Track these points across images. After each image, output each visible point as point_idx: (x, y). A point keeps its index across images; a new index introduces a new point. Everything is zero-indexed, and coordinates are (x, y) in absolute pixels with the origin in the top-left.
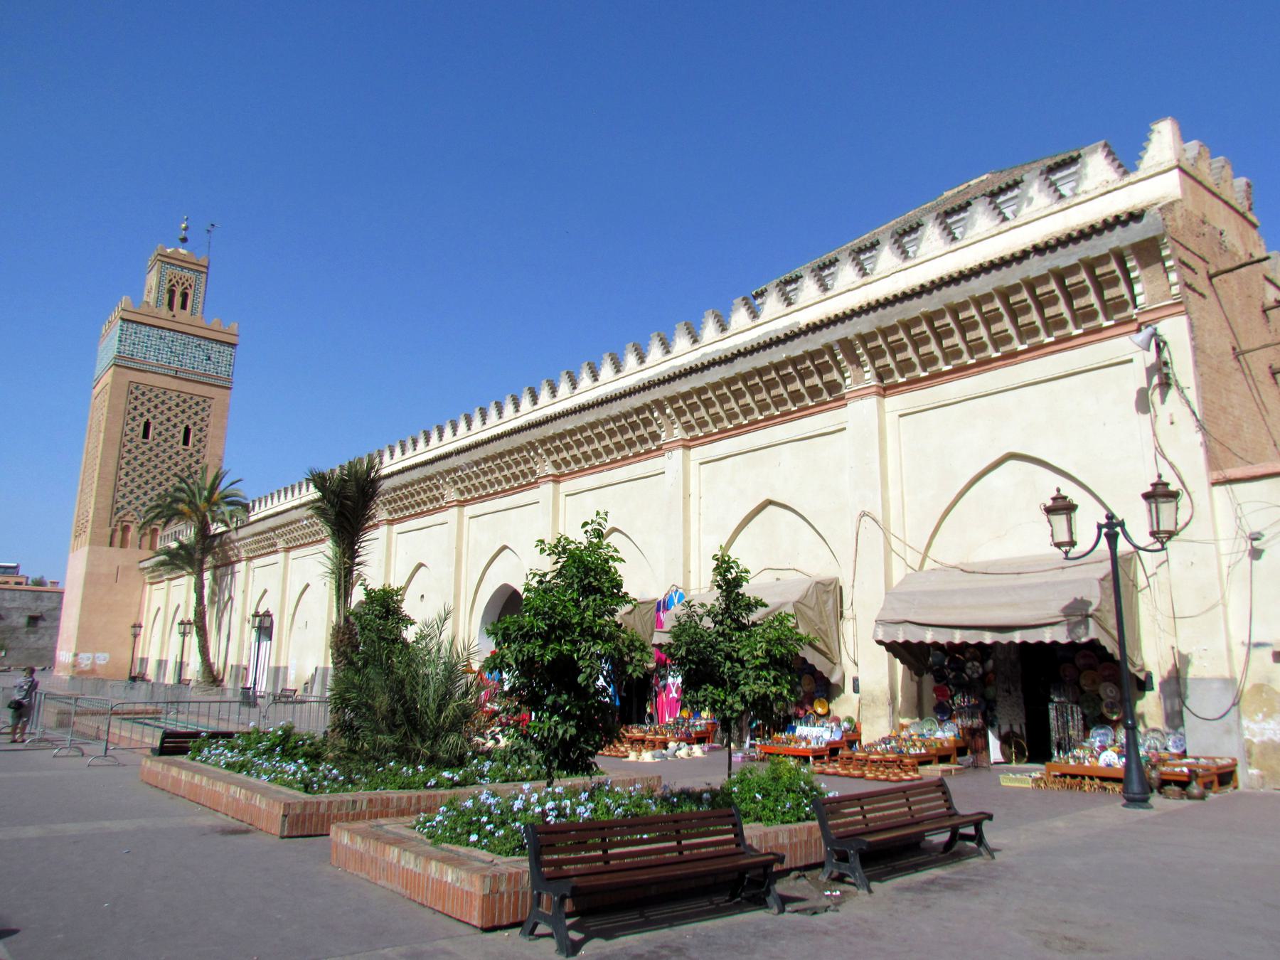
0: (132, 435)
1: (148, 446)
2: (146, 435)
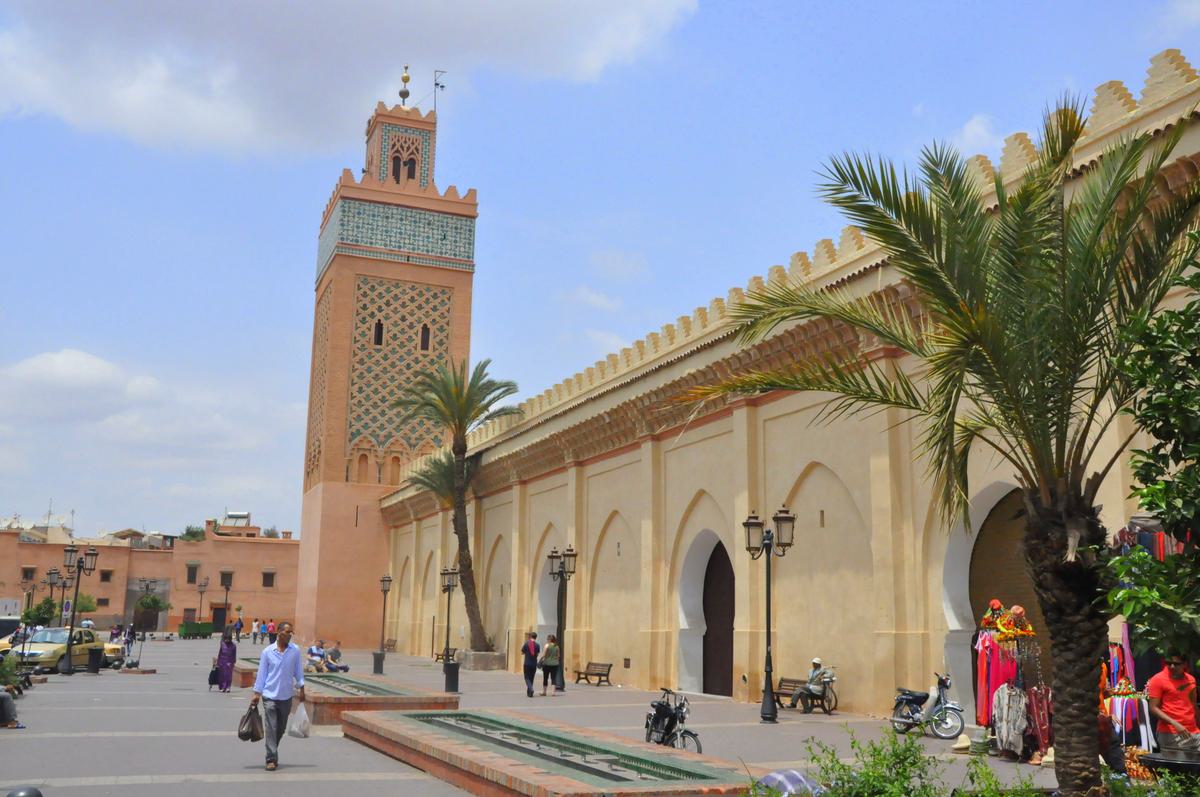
0: (363, 341)
1: (381, 354)
2: (379, 340)
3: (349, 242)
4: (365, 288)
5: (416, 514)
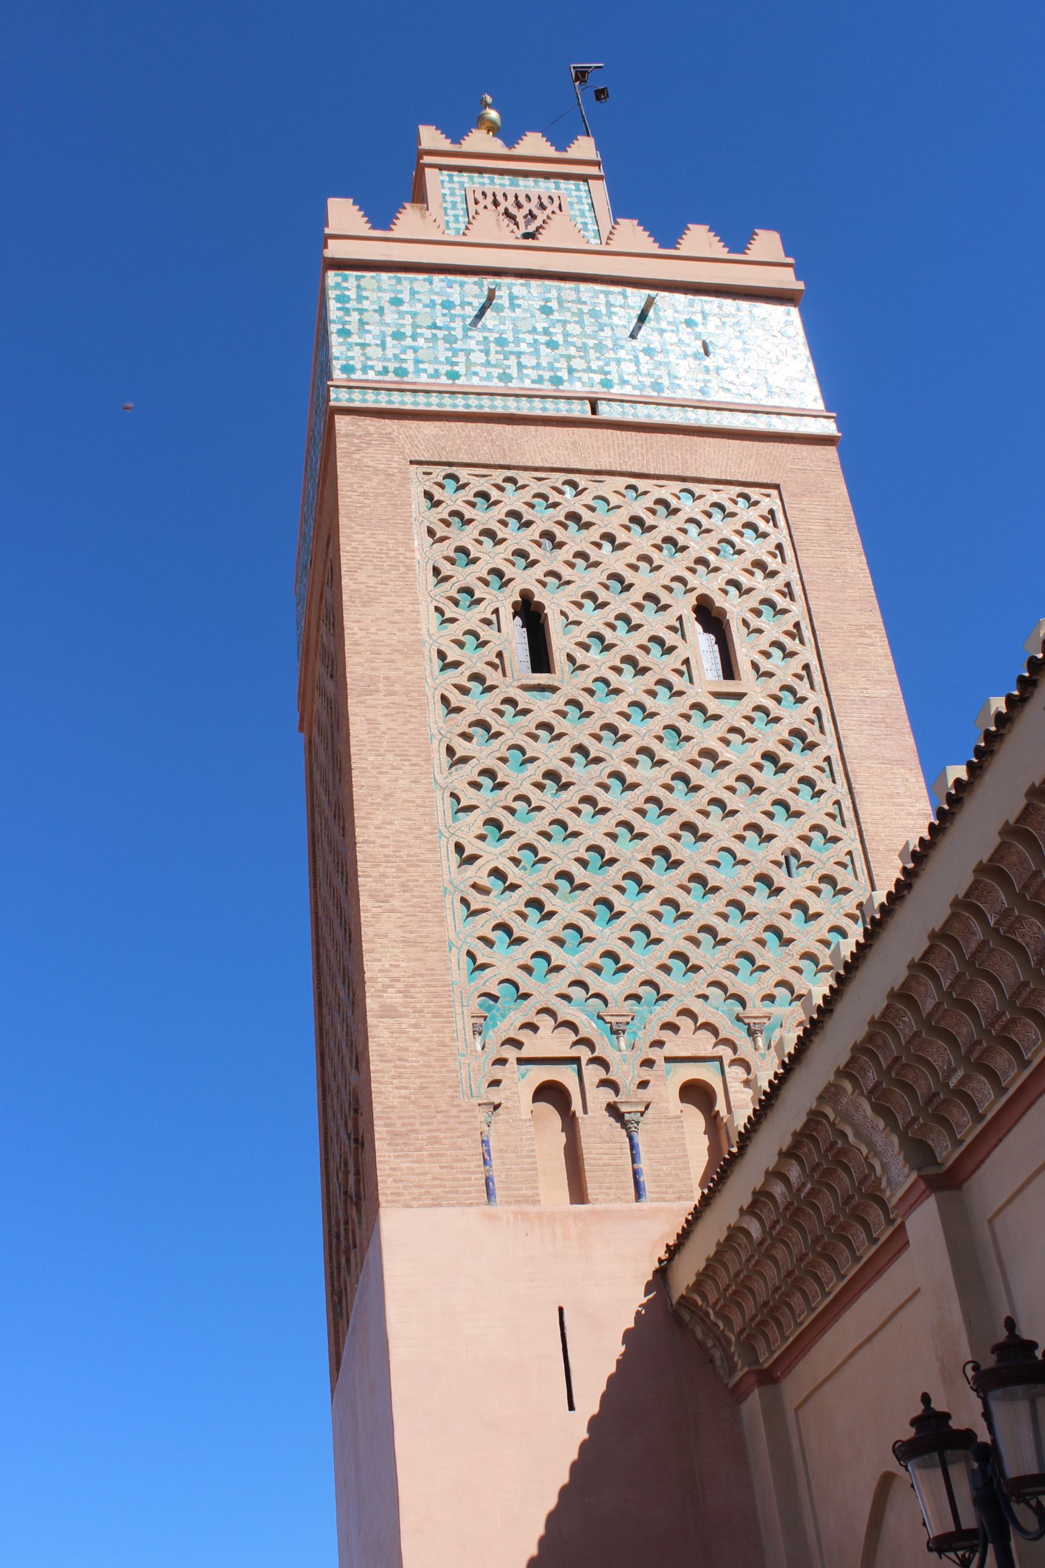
3: (371, 375)
4: (453, 500)
5: (919, 1151)
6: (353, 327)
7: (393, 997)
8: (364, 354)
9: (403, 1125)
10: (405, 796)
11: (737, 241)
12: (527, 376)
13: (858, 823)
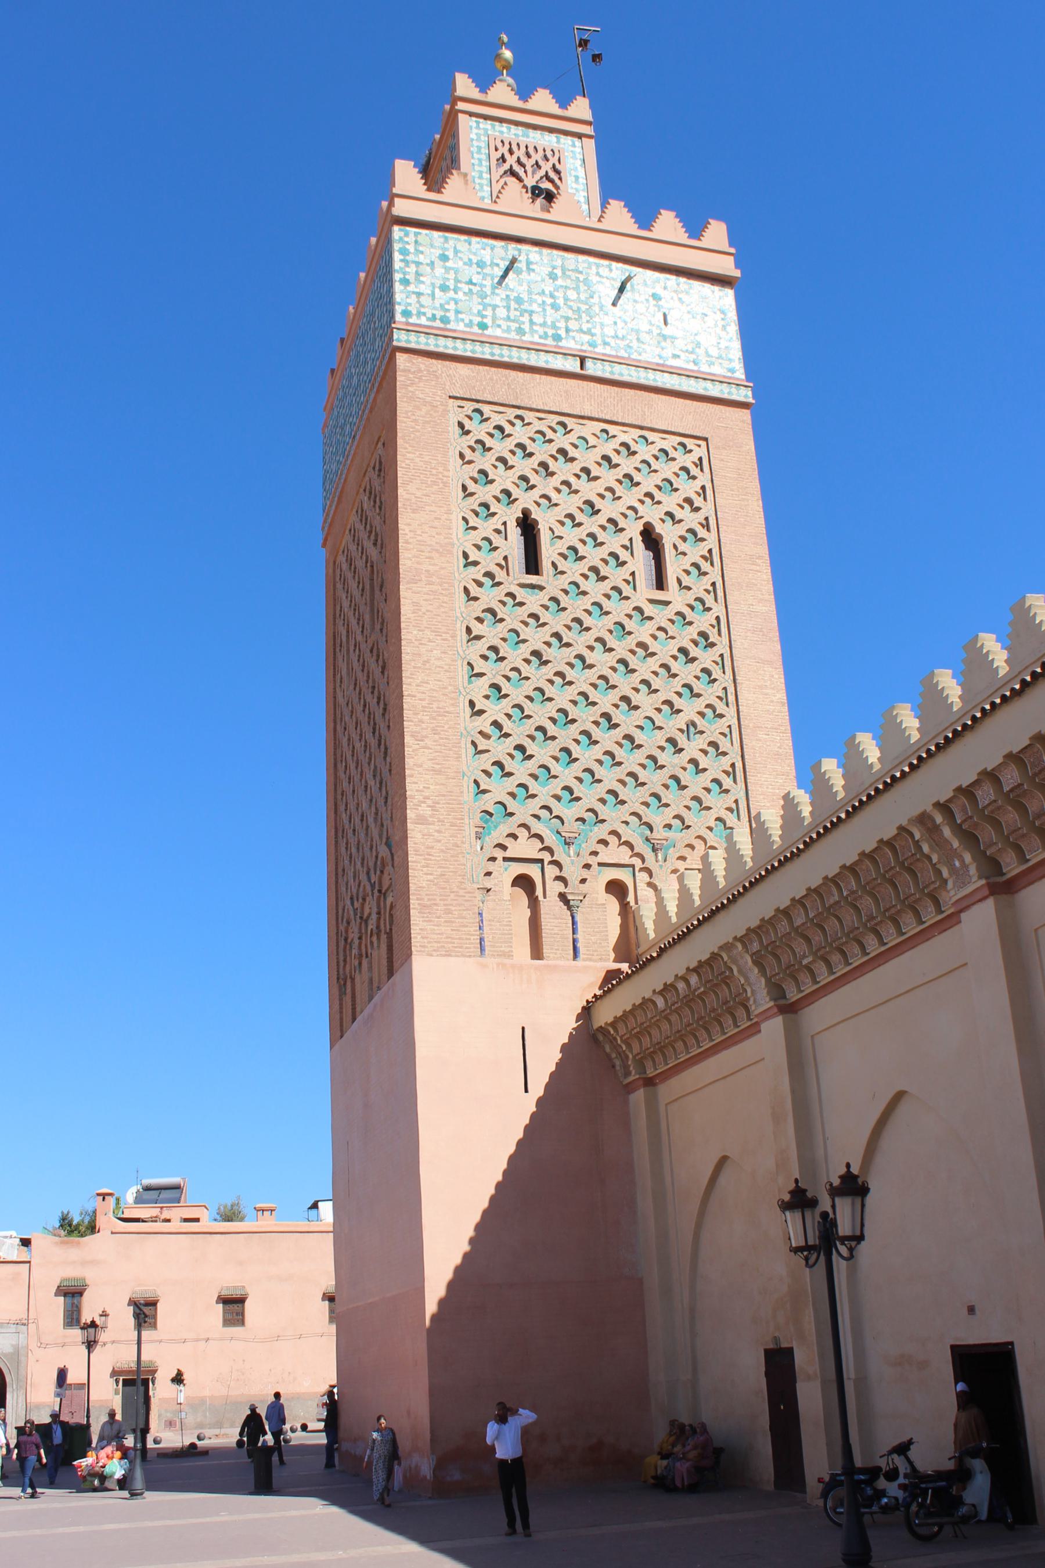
0: (488, 561)
3: (423, 321)
4: (479, 431)
5: (777, 991)
6: (411, 277)
7: (425, 810)
8: (418, 302)
9: (429, 900)
10: (438, 663)
11: (695, 229)
12: (536, 331)
13: (737, 706)
